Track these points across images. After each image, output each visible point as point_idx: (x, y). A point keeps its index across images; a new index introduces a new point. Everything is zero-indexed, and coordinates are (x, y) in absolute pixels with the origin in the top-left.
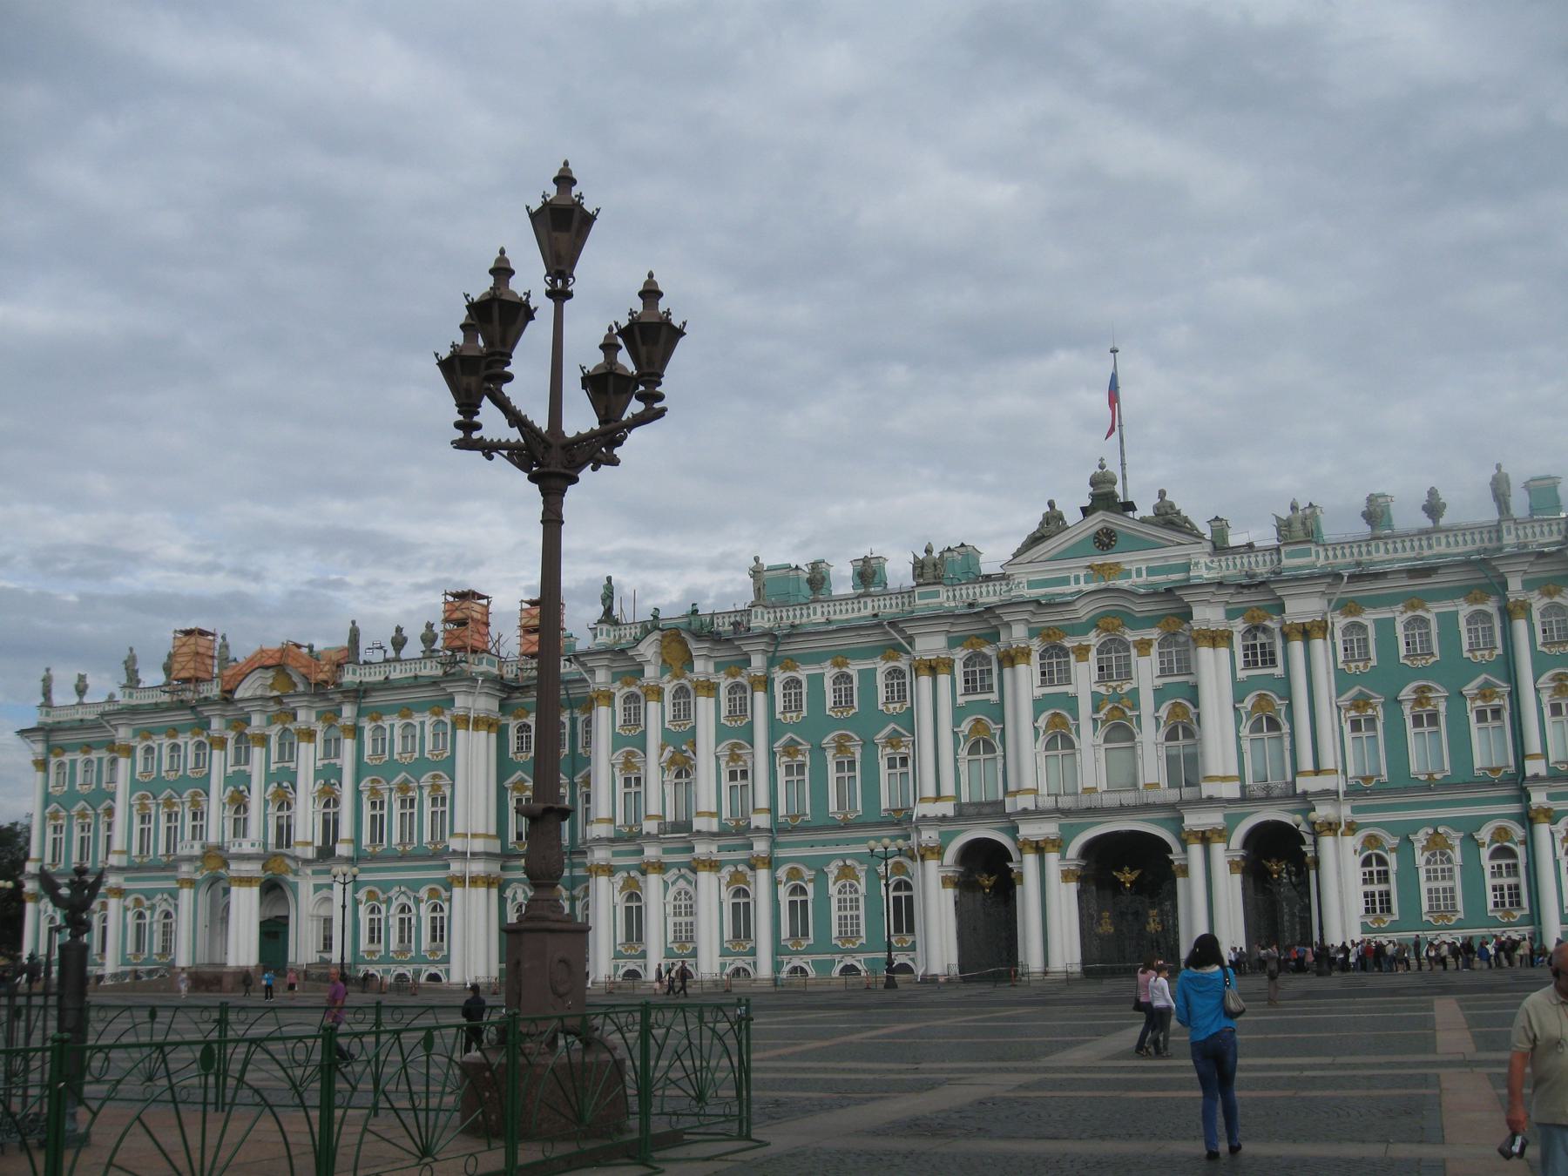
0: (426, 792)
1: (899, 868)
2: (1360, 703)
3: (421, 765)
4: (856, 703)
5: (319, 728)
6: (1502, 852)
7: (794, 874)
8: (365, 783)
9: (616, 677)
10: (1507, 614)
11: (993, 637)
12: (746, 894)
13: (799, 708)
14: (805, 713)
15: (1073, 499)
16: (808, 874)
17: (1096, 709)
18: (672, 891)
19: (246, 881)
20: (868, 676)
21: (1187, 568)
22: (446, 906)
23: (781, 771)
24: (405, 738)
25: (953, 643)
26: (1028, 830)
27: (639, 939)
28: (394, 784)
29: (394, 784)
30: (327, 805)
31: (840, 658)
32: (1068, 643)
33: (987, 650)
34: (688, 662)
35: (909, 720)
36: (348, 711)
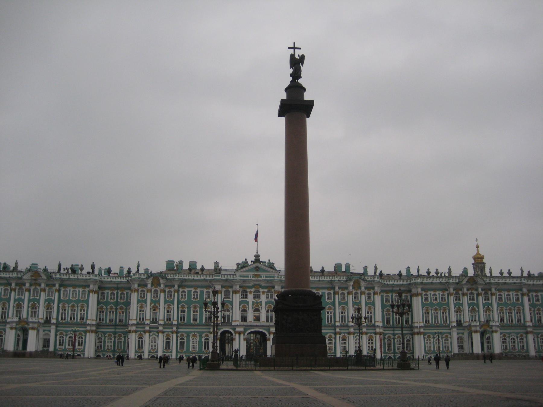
0: (79, 308)
1: (207, 335)
3: (78, 301)
5: (47, 288)
6: (330, 340)
7: (182, 335)
8: (61, 305)
9: (139, 286)
10: (335, 293)
11: (232, 287)
12: (169, 339)
13: (185, 298)
15: (251, 258)
16: (185, 335)
17: (253, 304)
18: (151, 337)
19: (33, 329)
20: (202, 292)
21: (274, 277)
22: (84, 337)
23: (180, 312)
24: (73, 294)
26: (238, 329)
27: (142, 348)
28: (70, 305)
29: (70, 305)
30: (48, 309)
31: (196, 287)
32: (248, 290)
34: (159, 285)
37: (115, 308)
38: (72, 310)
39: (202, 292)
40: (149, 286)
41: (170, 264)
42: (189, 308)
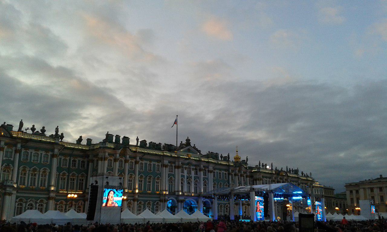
0: (41, 173)
1: (158, 203)
2: (215, 184)
4: (152, 170)
5: (6, 147)
6: (226, 209)
10: (229, 174)
11: (174, 163)
14: (144, 170)
17: (187, 178)
25: (169, 162)
29: (31, 169)
30: (5, 171)
31: (151, 160)
32: (184, 166)
33: (173, 165)
35: (160, 174)
36: (19, 146)
37: (67, 174)
38: (32, 175)
39: (154, 165)
40: (118, 155)
41: (109, 137)
42: (145, 178)
